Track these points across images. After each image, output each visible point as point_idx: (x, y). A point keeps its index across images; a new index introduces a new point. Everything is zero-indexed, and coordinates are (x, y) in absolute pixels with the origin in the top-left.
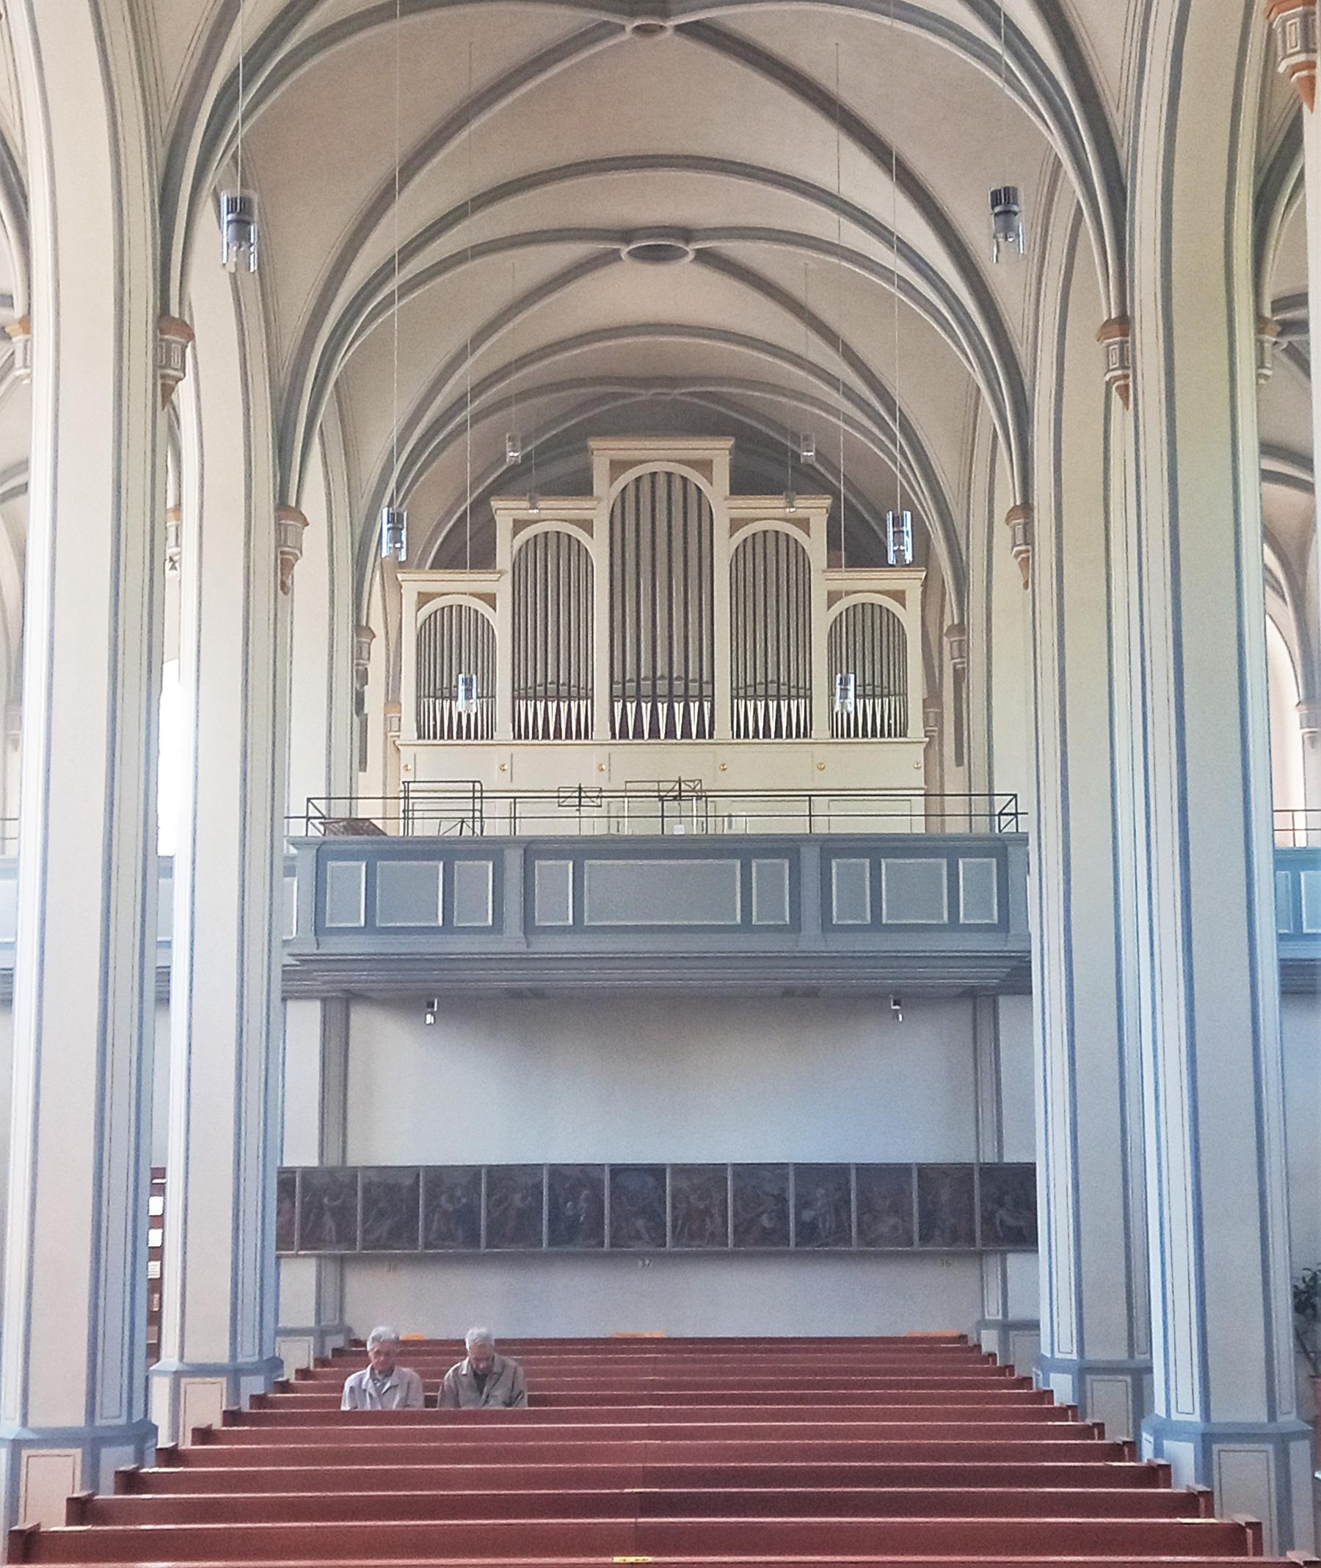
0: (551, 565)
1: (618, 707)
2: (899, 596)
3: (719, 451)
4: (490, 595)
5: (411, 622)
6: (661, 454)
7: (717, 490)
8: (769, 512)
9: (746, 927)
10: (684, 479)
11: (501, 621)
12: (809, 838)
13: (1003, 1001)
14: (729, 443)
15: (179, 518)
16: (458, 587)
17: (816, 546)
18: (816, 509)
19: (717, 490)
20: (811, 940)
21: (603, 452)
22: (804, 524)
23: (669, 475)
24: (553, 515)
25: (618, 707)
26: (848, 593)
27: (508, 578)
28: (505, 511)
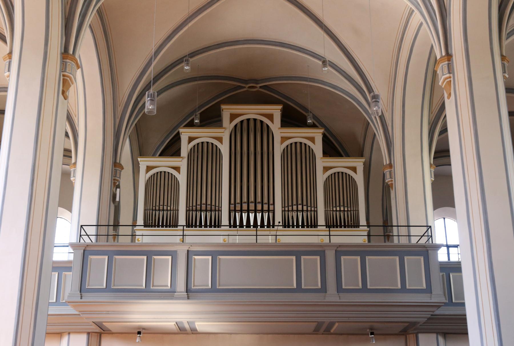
0: (204, 156)
1: (232, 214)
2: (354, 169)
3: (276, 111)
4: (178, 167)
5: (143, 178)
6: (251, 111)
7: (275, 126)
8: (298, 135)
9: (299, 289)
10: (262, 122)
11: (182, 178)
12: (330, 245)
13: (421, 336)
14: (280, 107)
15: (10, 58)
16: (164, 164)
17: (318, 148)
18: (318, 134)
19: (275, 126)
20: (332, 296)
21: (227, 110)
22: (312, 139)
23: (255, 120)
24: (205, 135)
25: (232, 214)
26: (331, 168)
27: (186, 160)
28: (185, 133)
